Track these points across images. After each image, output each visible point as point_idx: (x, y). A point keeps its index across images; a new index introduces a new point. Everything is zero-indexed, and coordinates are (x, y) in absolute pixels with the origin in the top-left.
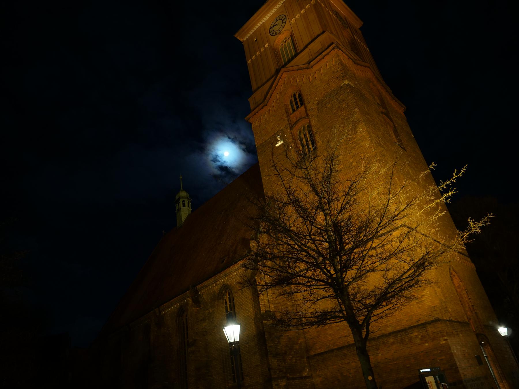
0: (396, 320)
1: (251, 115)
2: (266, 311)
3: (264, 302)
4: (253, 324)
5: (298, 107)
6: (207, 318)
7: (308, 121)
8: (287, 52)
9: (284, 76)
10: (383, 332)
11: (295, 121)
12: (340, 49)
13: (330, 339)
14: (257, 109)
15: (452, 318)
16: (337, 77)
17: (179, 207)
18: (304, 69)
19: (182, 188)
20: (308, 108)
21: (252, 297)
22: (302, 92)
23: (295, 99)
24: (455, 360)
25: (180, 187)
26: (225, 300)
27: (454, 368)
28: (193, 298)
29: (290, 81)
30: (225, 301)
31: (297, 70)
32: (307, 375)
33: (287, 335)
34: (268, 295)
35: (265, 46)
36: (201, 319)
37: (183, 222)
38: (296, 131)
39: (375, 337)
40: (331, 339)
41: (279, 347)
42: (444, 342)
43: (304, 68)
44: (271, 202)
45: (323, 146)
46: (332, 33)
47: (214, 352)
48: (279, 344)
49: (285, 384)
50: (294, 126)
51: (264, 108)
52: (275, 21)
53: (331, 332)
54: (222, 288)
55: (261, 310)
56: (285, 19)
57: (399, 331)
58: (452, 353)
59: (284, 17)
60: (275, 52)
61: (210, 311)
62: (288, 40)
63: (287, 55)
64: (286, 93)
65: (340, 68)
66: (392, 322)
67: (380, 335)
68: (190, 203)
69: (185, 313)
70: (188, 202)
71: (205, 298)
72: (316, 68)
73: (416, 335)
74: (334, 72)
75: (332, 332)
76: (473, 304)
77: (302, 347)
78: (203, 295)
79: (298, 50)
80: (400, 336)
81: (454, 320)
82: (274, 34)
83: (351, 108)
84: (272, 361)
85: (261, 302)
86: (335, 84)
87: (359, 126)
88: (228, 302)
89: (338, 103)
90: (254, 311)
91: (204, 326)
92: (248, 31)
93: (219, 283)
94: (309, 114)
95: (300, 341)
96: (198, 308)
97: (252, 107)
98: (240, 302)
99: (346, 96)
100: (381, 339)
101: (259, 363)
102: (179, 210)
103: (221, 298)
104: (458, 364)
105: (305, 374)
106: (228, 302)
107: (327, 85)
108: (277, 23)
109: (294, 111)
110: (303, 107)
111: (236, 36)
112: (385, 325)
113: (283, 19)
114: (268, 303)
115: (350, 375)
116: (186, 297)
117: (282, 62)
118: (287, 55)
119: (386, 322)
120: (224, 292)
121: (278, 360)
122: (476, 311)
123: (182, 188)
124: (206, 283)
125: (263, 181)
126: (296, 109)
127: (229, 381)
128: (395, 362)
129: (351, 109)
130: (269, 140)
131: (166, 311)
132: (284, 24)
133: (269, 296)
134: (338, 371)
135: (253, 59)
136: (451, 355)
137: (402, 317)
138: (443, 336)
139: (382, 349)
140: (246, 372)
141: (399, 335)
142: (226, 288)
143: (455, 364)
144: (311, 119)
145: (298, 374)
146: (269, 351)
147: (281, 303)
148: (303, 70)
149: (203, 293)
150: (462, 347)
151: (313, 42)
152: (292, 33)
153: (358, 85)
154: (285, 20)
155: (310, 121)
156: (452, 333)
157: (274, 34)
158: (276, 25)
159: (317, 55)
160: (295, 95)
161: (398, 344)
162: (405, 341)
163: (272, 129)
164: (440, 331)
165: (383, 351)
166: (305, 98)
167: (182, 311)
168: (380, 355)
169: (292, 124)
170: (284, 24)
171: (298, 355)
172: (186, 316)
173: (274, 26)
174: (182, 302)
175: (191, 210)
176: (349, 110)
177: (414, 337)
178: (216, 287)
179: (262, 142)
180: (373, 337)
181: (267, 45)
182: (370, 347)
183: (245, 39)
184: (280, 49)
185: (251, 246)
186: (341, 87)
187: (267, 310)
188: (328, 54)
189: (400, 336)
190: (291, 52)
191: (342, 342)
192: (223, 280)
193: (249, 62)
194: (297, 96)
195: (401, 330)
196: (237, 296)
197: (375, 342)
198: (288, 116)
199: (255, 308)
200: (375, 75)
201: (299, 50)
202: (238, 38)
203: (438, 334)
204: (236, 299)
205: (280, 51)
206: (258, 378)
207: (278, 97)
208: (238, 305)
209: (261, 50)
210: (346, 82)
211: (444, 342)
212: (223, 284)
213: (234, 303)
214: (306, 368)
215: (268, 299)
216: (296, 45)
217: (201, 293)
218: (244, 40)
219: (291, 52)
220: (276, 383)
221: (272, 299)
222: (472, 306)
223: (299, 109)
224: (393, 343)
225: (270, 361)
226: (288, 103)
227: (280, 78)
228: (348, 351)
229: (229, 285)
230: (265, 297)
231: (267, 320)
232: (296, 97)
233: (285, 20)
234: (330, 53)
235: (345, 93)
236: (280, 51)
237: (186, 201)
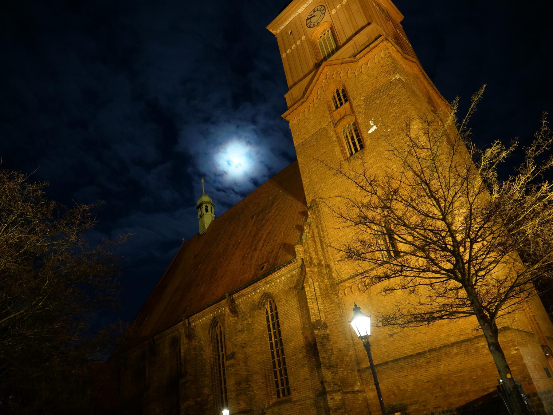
0: (460, 329)
1: (288, 112)
2: (316, 320)
3: (314, 310)
4: (301, 335)
5: (341, 104)
6: (245, 329)
7: (354, 119)
8: (326, 46)
9: (326, 70)
10: (445, 342)
11: (338, 119)
12: (389, 42)
13: (384, 351)
14: (296, 106)
15: (519, 327)
16: (387, 71)
17: (201, 213)
18: (349, 62)
19: (204, 193)
20: (354, 104)
21: (298, 306)
22: (346, 87)
23: (338, 95)
24: (528, 371)
25: (203, 192)
26: (265, 310)
27: (527, 379)
28: (230, 307)
29: (333, 75)
30: (265, 311)
31: (341, 64)
32: (359, 390)
33: (337, 347)
34: (318, 303)
35: (302, 39)
37: (206, 229)
38: (340, 129)
39: (436, 348)
40: (385, 351)
41: (332, 359)
42: (515, 352)
43: (349, 61)
44: (313, 205)
45: (372, 144)
46: (378, 24)
47: (255, 365)
48: (332, 355)
49: (340, 398)
50: (339, 123)
51: (304, 104)
52: (313, 12)
53: (385, 344)
54: (263, 297)
55: (312, 319)
56: (324, 10)
57: (464, 341)
58: (524, 364)
59: (323, 8)
60: (313, 46)
61: (249, 322)
62: (327, 33)
63: (327, 48)
64: (328, 89)
65: (390, 61)
66: (455, 331)
67: (442, 346)
68: (213, 209)
69: (219, 325)
70: (212, 208)
72: (362, 62)
73: (483, 345)
74: (382, 66)
75: (386, 343)
76: (534, 314)
77: (353, 360)
78: (240, 304)
79: (340, 43)
80: (465, 347)
81: (521, 329)
82: (312, 26)
83: (404, 103)
84: (326, 373)
85: (310, 310)
86: (385, 78)
87: (413, 123)
88: (269, 312)
89: (388, 98)
90: (302, 321)
91: (243, 338)
92: (282, 23)
93: (259, 291)
94: (356, 110)
95: (350, 353)
96: (236, 319)
97: (289, 104)
98: (285, 311)
99: (398, 92)
100: (443, 350)
101: (308, 377)
102: (201, 216)
103: (261, 307)
104: (531, 375)
105: (357, 388)
106: (269, 312)
107: (375, 80)
108: (315, 14)
109: (337, 107)
110: (348, 103)
111: (268, 28)
112: (447, 335)
113: (321, 10)
114: (318, 312)
115: (408, 389)
117: (321, 56)
118: (327, 48)
119: (448, 332)
120: (264, 301)
121: (332, 372)
122: (537, 322)
123: (204, 193)
124: (244, 291)
125: (304, 183)
126: (339, 105)
127: (273, 396)
128: (460, 375)
129: (404, 104)
130: (310, 139)
132: (322, 15)
133: (319, 304)
134: (394, 384)
135: (288, 52)
136: (524, 365)
137: (466, 326)
138: (514, 346)
139: (444, 360)
140: (293, 386)
141: (464, 346)
142: (267, 296)
143: (529, 375)
144: (358, 117)
145: (350, 388)
146: (322, 362)
147: (330, 312)
148: (348, 64)
150: (532, 358)
151: (359, 34)
152: (333, 25)
153: (408, 80)
154: (323, 12)
155: (356, 118)
156: (522, 343)
157: (312, 26)
158: (314, 16)
159: (363, 47)
160: (337, 91)
161: (463, 355)
162: (471, 351)
163: (313, 127)
164: (511, 340)
165: (446, 363)
166: (350, 94)
167: (215, 322)
168: (442, 366)
169: (336, 121)
170: (322, 15)
171: (349, 368)
172: (220, 328)
173: (311, 17)
174: (216, 313)
175: (214, 216)
176: (401, 106)
177: (481, 347)
178: (256, 296)
179: (301, 141)
180: (434, 347)
181: (303, 38)
182: (430, 358)
183: (278, 31)
184: (318, 42)
185: (296, 251)
186: (392, 82)
187: (317, 319)
188: (376, 46)
189: (465, 347)
190: (331, 45)
191: (397, 354)
192: (263, 289)
193: (284, 56)
194: (340, 92)
195: (465, 340)
196: (281, 305)
197: (436, 353)
198: (331, 113)
199: (302, 317)
200: (421, 71)
201: (341, 42)
202: (271, 30)
203: (509, 343)
204: (279, 308)
205: (318, 44)
206: (308, 392)
207: (319, 93)
208: (283, 314)
209: (297, 44)
210: (398, 76)
211: (515, 352)
212: (264, 293)
213: (277, 312)
214: (357, 382)
215: (318, 307)
216: (338, 38)
217: (238, 303)
218: (277, 33)
219: (331, 45)
220: (331, 397)
221: (322, 307)
222: (534, 316)
223: (343, 106)
224: (457, 354)
225: (324, 373)
226: (331, 99)
227: (321, 73)
228: (406, 363)
229: (272, 293)
230: (314, 305)
231: (319, 330)
232: (339, 93)
233: (323, 12)
234: (378, 46)
235: (396, 88)
236: (318, 44)
237: (209, 206)
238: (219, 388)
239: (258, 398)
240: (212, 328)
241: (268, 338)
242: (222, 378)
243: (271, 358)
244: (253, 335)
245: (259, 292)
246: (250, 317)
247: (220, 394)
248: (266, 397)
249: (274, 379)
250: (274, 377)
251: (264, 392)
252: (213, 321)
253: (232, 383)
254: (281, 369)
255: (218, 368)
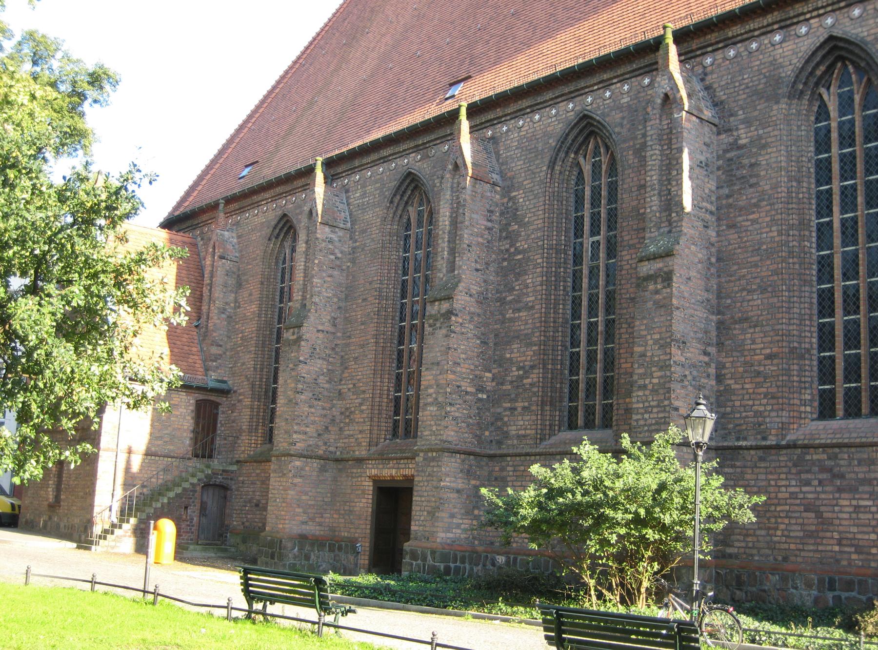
36: (701, 162)
47: (745, 293)
61: (739, 137)
71: (715, 86)
78: (706, 74)
116: (615, 81)
131: (505, 128)
149: (709, 69)
178: (789, 46)
229: (869, 39)
238: (567, 353)
239: (737, 403)
240: (567, 153)
241: (814, 207)
242: (584, 322)
243: (814, 278)
244: (751, 186)
245: (807, 34)
246: (748, 122)
247: (567, 372)
248: (775, 407)
249: (815, 352)
250: (815, 346)
251: (774, 390)
252: (572, 129)
253: (657, 336)
254: (857, 323)
255: (570, 289)
